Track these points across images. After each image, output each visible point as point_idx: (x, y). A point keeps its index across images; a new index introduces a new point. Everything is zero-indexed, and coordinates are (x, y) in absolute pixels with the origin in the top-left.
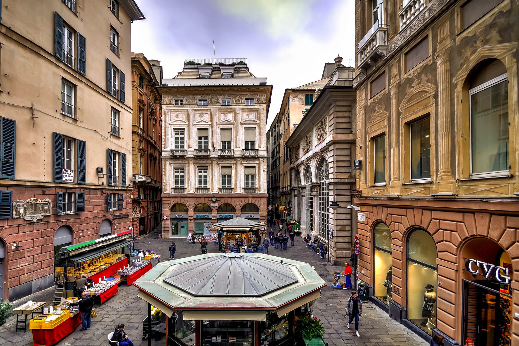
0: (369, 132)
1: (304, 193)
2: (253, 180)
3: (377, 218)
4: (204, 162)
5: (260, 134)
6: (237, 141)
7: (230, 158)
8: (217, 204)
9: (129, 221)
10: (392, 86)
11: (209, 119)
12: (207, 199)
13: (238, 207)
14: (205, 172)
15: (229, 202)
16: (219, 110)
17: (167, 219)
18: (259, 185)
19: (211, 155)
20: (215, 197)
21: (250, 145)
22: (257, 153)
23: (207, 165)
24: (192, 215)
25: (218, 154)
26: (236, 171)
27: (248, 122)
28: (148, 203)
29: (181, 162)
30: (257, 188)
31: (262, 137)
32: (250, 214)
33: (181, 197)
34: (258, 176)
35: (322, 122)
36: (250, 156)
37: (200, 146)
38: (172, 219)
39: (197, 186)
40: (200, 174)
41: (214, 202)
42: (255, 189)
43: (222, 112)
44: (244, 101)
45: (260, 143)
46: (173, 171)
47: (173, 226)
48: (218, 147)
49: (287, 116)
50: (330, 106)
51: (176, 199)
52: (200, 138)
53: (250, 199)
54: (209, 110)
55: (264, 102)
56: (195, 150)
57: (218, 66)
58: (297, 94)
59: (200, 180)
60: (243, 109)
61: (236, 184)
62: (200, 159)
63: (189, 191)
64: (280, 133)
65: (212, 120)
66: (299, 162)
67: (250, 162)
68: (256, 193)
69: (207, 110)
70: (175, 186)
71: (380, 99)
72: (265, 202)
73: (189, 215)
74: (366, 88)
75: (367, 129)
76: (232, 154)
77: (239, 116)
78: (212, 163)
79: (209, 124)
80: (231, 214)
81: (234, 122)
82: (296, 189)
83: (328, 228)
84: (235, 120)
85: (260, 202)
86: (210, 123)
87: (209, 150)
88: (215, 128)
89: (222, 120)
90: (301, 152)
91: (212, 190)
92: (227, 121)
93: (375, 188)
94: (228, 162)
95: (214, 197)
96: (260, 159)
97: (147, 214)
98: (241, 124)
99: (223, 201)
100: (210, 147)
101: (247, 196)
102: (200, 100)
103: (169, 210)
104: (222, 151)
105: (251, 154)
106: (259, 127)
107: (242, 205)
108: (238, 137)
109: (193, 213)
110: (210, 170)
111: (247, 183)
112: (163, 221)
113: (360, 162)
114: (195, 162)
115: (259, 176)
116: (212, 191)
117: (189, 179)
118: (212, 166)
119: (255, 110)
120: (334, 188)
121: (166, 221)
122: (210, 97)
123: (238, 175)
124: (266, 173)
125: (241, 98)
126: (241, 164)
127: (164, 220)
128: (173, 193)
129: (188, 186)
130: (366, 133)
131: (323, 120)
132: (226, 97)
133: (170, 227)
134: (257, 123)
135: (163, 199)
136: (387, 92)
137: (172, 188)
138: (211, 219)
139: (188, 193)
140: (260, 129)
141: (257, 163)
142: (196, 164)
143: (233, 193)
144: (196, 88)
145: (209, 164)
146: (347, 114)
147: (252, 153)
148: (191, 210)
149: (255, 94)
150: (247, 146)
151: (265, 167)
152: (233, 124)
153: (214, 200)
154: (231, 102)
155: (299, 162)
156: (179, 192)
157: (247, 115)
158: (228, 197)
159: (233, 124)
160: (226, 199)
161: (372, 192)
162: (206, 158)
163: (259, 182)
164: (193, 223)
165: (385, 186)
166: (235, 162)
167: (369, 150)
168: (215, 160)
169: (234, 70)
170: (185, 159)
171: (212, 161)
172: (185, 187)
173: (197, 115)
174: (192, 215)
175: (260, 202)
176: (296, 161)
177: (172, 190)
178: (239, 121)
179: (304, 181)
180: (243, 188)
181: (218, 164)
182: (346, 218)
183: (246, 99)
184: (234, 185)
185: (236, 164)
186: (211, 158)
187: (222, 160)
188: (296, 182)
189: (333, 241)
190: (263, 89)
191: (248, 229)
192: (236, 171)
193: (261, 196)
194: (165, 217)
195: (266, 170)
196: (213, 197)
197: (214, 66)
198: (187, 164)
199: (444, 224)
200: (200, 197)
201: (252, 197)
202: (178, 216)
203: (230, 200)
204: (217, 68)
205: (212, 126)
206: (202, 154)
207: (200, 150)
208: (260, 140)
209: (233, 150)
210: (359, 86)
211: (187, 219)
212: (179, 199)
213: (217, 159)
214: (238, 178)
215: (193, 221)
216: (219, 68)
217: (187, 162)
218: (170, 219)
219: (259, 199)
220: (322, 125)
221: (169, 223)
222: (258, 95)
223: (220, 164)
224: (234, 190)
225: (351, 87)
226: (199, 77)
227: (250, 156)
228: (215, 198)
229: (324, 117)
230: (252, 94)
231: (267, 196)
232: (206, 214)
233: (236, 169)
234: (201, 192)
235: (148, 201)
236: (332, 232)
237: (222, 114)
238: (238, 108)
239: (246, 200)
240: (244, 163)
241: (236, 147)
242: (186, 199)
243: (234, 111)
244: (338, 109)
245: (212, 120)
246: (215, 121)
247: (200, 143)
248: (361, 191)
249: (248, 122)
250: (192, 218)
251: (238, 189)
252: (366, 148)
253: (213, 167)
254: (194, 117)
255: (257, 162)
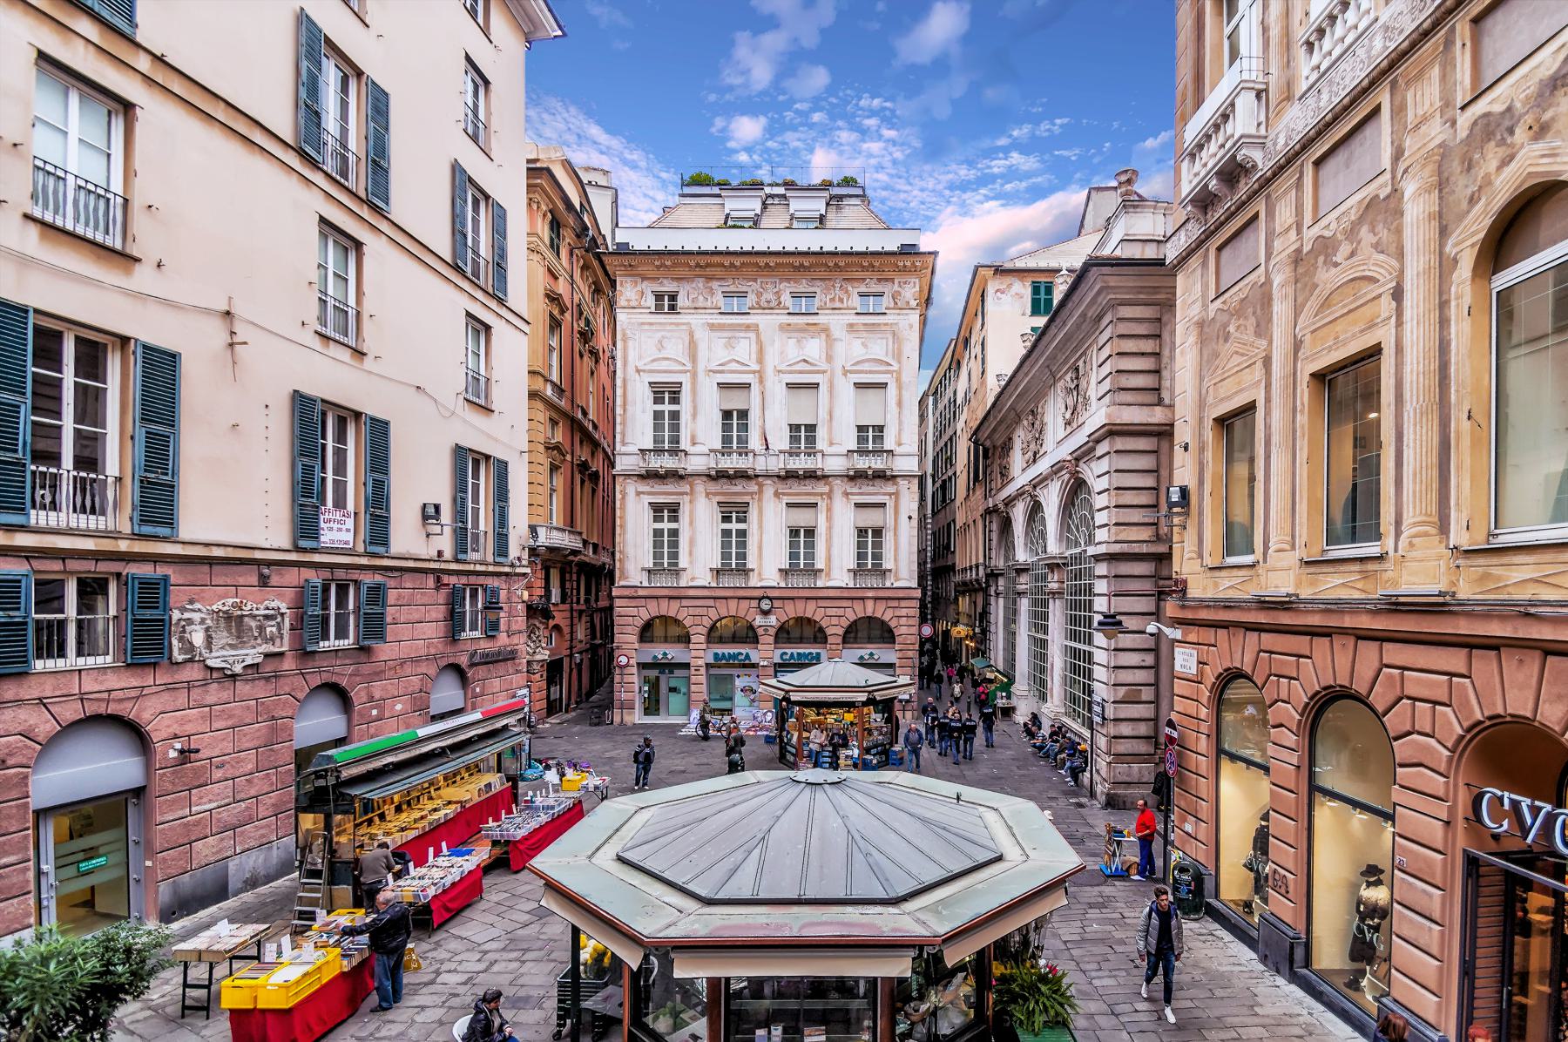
0: (1210, 400)
1: (1024, 587)
2: (878, 545)
3: (1227, 664)
4: (738, 489)
5: (900, 404)
6: (834, 423)
7: (811, 475)
8: (773, 620)
9: (518, 672)
10: (1278, 259)
11: (754, 356)
12: (744, 604)
13: (835, 630)
14: (739, 520)
15: (809, 615)
16: (786, 328)
17: (627, 665)
18: (896, 560)
19: (758, 468)
20: (768, 598)
21: (870, 436)
22: (889, 464)
23: (746, 499)
24: (701, 653)
25: (776, 464)
26: (829, 519)
27: (866, 367)
28: (575, 614)
29: (670, 488)
30: (890, 571)
31: (906, 412)
32: (869, 651)
33: (671, 598)
34: (892, 533)
35: (1077, 369)
36: (870, 472)
37: (726, 440)
38: (642, 666)
39: (717, 563)
40: (727, 526)
41: (766, 613)
42: (884, 573)
43: (793, 335)
44: (856, 301)
45: (900, 430)
46: (648, 514)
47: (646, 688)
48: (780, 441)
49: (979, 348)
50: (1100, 318)
51: (654, 603)
52: (727, 415)
53: (870, 604)
54: (754, 328)
55: (913, 303)
56: (711, 451)
57: (780, 190)
58: (1008, 279)
59: (726, 545)
60: (851, 325)
61: (829, 559)
62: (725, 480)
63: (693, 579)
64: (959, 402)
65: (760, 360)
66: (1010, 490)
67: (870, 489)
68: (888, 584)
69: (748, 328)
70: (652, 561)
71: (1243, 300)
72: (912, 612)
73: (694, 653)
74: (1204, 264)
75: (1204, 391)
76: (820, 466)
77: (840, 349)
78: (761, 492)
79: (754, 372)
80: (814, 651)
81: (824, 366)
82: (1002, 574)
83: (1091, 692)
84: (829, 358)
85: (898, 613)
86: (756, 367)
87: (753, 451)
88: (769, 384)
89: (790, 357)
90: (1017, 459)
91: (760, 574)
92: (805, 361)
93: (1224, 573)
94: (808, 489)
95: (766, 599)
96: (899, 479)
97: (571, 648)
98: (845, 372)
99: (791, 611)
100: (755, 443)
101: (860, 594)
102: (727, 295)
103: (634, 638)
104: (791, 454)
105: (873, 466)
106: (898, 380)
107: (846, 623)
108: (836, 414)
109: (704, 646)
110: (753, 514)
111: (861, 556)
112: (617, 671)
113: (1184, 492)
114: (713, 487)
115: (895, 534)
116: (762, 580)
117: (692, 542)
118: (760, 500)
119: (888, 328)
120: (1109, 571)
121: (626, 671)
122: (756, 286)
123: (836, 531)
124: (915, 522)
125: (847, 292)
126: (846, 494)
127: (621, 667)
128: (646, 584)
129: (691, 563)
130: (1202, 404)
131: (1081, 363)
132: (803, 287)
133: (637, 690)
134: (890, 368)
135: (617, 602)
136: (1263, 280)
137: (643, 569)
138: (754, 666)
139: (691, 584)
140: (900, 388)
141: (890, 494)
142: (716, 494)
143: (819, 584)
144: (717, 259)
145: (751, 494)
146: (1148, 346)
147: (877, 463)
148: (698, 639)
149: (887, 280)
150: (862, 440)
151: (915, 505)
152: (824, 372)
153: (765, 605)
154: (817, 302)
155: (1010, 490)
156: (664, 581)
157: (863, 344)
158: (807, 598)
159: (824, 372)
160: (800, 604)
161: (1216, 585)
162: (742, 475)
163: (896, 550)
164: (703, 679)
165: (1252, 566)
166: (826, 489)
167: (1209, 455)
168: (769, 482)
169: (828, 204)
170: (681, 477)
171: (761, 486)
172: (681, 565)
173: (719, 340)
174: (701, 653)
175: (898, 613)
176: (1003, 486)
177: (645, 574)
178: (839, 363)
179: (1025, 551)
180: (849, 570)
181: (777, 494)
182: (1143, 664)
183: (861, 295)
184: (823, 560)
185: (830, 495)
186: (757, 476)
187: (790, 482)
188: (1003, 552)
189: (1105, 732)
190: (908, 264)
191: (863, 697)
192: (829, 519)
193: (901, 594)
194: (623, 660)
195: (915, 515)
196: (763, 598)
197: (768, 190)
198: (686, 494)
199: (1416, 683)
200: (726, 598)
201: (876, 599)
202: (660, 657)
203: (811, 605)
204: (778, 196)
205: (760, 374)
206: (732, 463)
207: (726, 451)
208: (900, 423)
209: (822, 451)
210: (1184, 259)
211: (687, 666)
212: (664, 603)
213: (776, 479)
214: (835, 540)
215: (703, 671)
216: (784, 196)
217: (687, 488)
218: (638, 664)
219: (895, 603)
220: (1077, 378)
221: (635, 679)
222: (896, 281)
223: (784, 494)
224: (823, 574)
225: (1160, 263)
226: (726, 223)
227: (870, 472)
228: (768, 602)
229: (1084, 353)
230: (879, 280)
231: (918, 594)
232: (744, 652)
233: (829, 510)
234: (727, 581)
235: (572, 610)
236: (1103, 707)
237: (792, 342)
238: (836, 322)
239: (858, 606)
240: (852, 494)
241: (831, 444)
242: (685, 602)
243: (826, 330)
244: (1123, 328)
245: (760, 360)
246: (772, 360)
247: (726, 428)
248: (1185, 582)
249: (866, 367)
250: (701, 662)
251: (835, 573)
252: (1202, 450)
253: (765, 504)
254: (710, 348)
255: (890, 488)
